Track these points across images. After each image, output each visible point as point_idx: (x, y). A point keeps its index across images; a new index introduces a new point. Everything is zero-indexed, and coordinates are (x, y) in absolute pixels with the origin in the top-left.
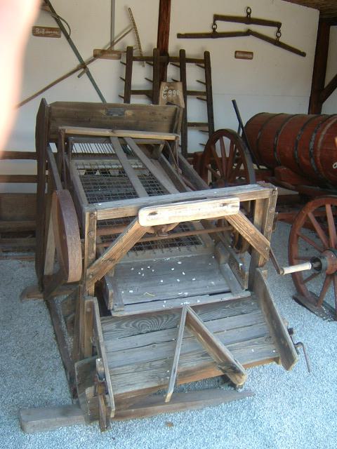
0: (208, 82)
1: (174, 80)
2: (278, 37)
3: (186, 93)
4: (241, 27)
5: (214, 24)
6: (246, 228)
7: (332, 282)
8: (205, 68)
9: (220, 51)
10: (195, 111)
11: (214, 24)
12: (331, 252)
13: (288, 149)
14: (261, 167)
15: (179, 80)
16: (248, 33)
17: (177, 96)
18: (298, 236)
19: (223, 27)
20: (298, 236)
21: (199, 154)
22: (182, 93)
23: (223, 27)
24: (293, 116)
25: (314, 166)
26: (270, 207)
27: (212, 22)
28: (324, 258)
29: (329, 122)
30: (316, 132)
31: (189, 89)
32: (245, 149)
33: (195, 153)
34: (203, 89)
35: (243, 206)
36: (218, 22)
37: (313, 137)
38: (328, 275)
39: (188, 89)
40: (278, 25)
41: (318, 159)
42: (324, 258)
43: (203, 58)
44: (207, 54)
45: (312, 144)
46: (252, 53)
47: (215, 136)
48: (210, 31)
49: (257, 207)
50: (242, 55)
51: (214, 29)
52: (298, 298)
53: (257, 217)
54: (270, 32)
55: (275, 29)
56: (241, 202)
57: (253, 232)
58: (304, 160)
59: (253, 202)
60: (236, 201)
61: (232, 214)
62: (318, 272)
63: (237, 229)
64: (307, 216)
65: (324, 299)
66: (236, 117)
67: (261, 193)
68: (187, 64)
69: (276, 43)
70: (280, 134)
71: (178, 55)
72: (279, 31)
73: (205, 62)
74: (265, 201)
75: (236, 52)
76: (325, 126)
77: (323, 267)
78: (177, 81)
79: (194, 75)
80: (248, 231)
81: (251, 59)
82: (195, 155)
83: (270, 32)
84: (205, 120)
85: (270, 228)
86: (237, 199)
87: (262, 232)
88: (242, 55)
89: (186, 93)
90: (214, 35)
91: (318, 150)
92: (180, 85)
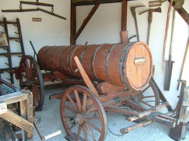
0: (20, 33)
1: (2, 32)
2: (53, 11)
3: (9, 39)
4: (35, 7)
5: (21, 5)
6: (14, 119)
7: (82, 128)
8: (17, 26)
9: (25, 18)
10: (15, 47)
11: (21, 5)
12: (79, 114)
13: (57, 63)
14: (48, 72)
15: (4, 32)
16: (38, 9)
17: (4, 40)
18: (64, 107)
19: (25, 7)
20: (64, 107)
21: (17, 68)
22: (6, 39)
23: (25, 7)
24: (59, 47)
25: (70, 70)
26: (29, 104)
27: (20, 4)
28: (76, 117)
29: (75, 49)
30: (69, 54)
31: (10, 37)
32: (37, 64)
33: (15, 67)
34: (17, 36)
35: (9, 107)
36: (22, 5)
37: (68, 56)
38: (79, 125)
39: (9, 37)
40: (52, 6)
41: (71, 67)
42: (76, 117)
43: (16, 22)
44: (18, 20)
45: (68, 60)
46: (41, 19)
47: (24, 58)
48: (19, 9)
49: (21, 105)
50: (36, 20)
51: (21, 8)
52: (68, 138)
53: (22, 111)
54: (49, 9)
55: (51, 8)
56: (7, 105)
57: (20, 121)
58: (65, 68)
59: (19, 103)
60: (5, 105)
61: (2, 113)
62: (74, 125)
63: (9, 121)
64: (67, 96)
65: (80, 136)
66: (32, 49)
67: (21, 97)
68: (8, 25)
69: (52, 14)
70: (53, 56)
71: (3, 21)
72: (53, 9)
73: (17, 23)
74: (25, 101)
75: (33, 18)
76: (73, 51)
77: (76, 122)
78: (3, 33)
79: (12, 30)
80: (16, 121)
81: (41, 21)
82: (15, 68)
83: (49, 9)
84: (20, 51)
85: (31, 116)
86: (4, 103)
87: (27, 120)
88: (36, 20)
89: (9, 39)
90: (21, 10)
91: (71, 62)
92: (5, 35)
